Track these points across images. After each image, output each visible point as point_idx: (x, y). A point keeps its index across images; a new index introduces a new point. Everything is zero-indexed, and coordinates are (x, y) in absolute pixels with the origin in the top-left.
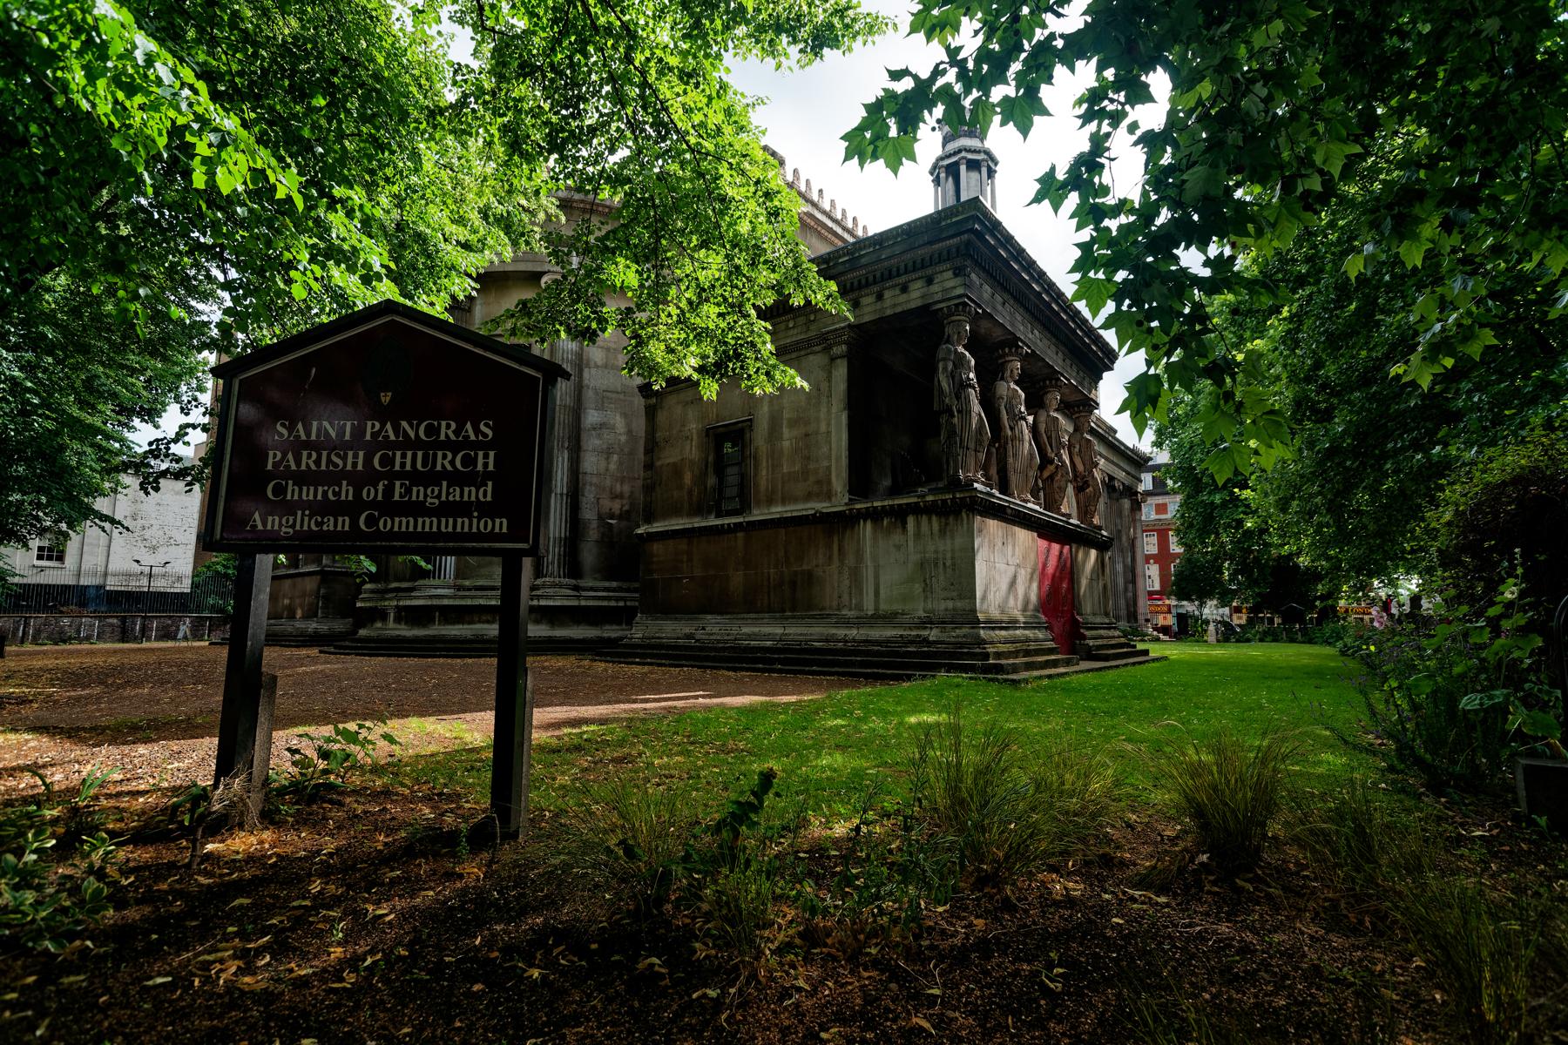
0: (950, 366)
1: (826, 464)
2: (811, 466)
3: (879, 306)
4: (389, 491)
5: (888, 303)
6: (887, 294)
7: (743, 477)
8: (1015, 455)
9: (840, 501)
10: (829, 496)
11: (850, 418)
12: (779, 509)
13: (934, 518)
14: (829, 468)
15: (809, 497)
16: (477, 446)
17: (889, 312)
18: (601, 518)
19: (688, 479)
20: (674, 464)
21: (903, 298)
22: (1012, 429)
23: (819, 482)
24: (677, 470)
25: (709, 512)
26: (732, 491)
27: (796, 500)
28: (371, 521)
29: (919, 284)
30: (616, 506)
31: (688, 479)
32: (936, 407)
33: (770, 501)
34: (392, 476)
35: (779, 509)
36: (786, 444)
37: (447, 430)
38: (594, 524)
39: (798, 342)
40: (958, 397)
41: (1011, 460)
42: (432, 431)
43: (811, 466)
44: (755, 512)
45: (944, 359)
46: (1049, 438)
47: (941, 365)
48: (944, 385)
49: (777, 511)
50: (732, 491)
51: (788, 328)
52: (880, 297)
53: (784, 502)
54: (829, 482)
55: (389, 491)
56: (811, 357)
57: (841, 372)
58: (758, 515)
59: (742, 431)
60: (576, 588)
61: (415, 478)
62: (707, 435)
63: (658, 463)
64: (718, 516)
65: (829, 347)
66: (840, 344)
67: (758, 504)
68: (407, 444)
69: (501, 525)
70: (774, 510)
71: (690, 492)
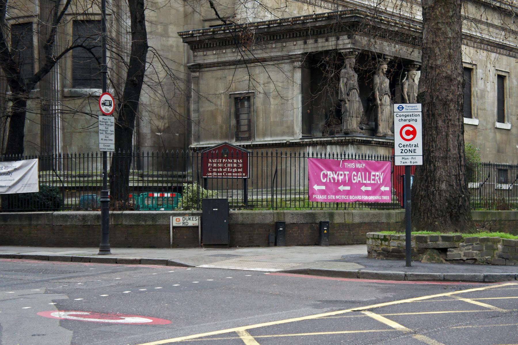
0: (345, 80)
1: (291, 119)
2: (284, 119)
3: (315, 45)
4: (227, 170)
5: (320, 45)
6: (320, 40)
7: (249, 121)
8: (382, 113)
9: (297, 137)
10: (293, 134)
11: (303, 97)
12: (269, 139)
13: (338, 147)
14: (293, 121)
15: (283, 134)
16: (240, 163)
17: (320, 49)
18: (152, 132)
19: (219, 120)
20: (212, 111)
21: (326, 44)
22: (381, 100)
23: (288, 127)
24: (213, 115)
25: (232, 138)
26: (244, 128)
27: (277, 135)
28: (225, 174)
29: (334, 39)
30: (161, 124)
31: (219, 120)
32: (339, 98)
33: (264, 135)
34: (227, 167)
35: (269, 139)
36: (272, 107)
37: (235, 161)
38: (149, 136)
39: (277, 57)
40: (348, 95)
41: (380, 115)
42: (233, 161)
43: (284, 119)
44: (257, 139)
45: (343, 77)
46: (409, 96)
47: (341, 79)
48: (343, 89)
49: (269, 140)
50: (244, 128)
51: (272, 48)
52: (316, 41)
53: (271, 136)
54: (293, 128)
55: (227, 170)
56: (283, 65)
57: (298, 75)
58: (258, 141)
59: (249, 97)
60: (142, 176)
61: (231, 168)
62: (230, 98)
63: (201, 110)
64: (237, 140)
65: (293, 62)
66: (298, 61)
67: (258, 136)
68: (230, 163)
69: (244, 174)
70: (266, 139)
71: (221, 127)
